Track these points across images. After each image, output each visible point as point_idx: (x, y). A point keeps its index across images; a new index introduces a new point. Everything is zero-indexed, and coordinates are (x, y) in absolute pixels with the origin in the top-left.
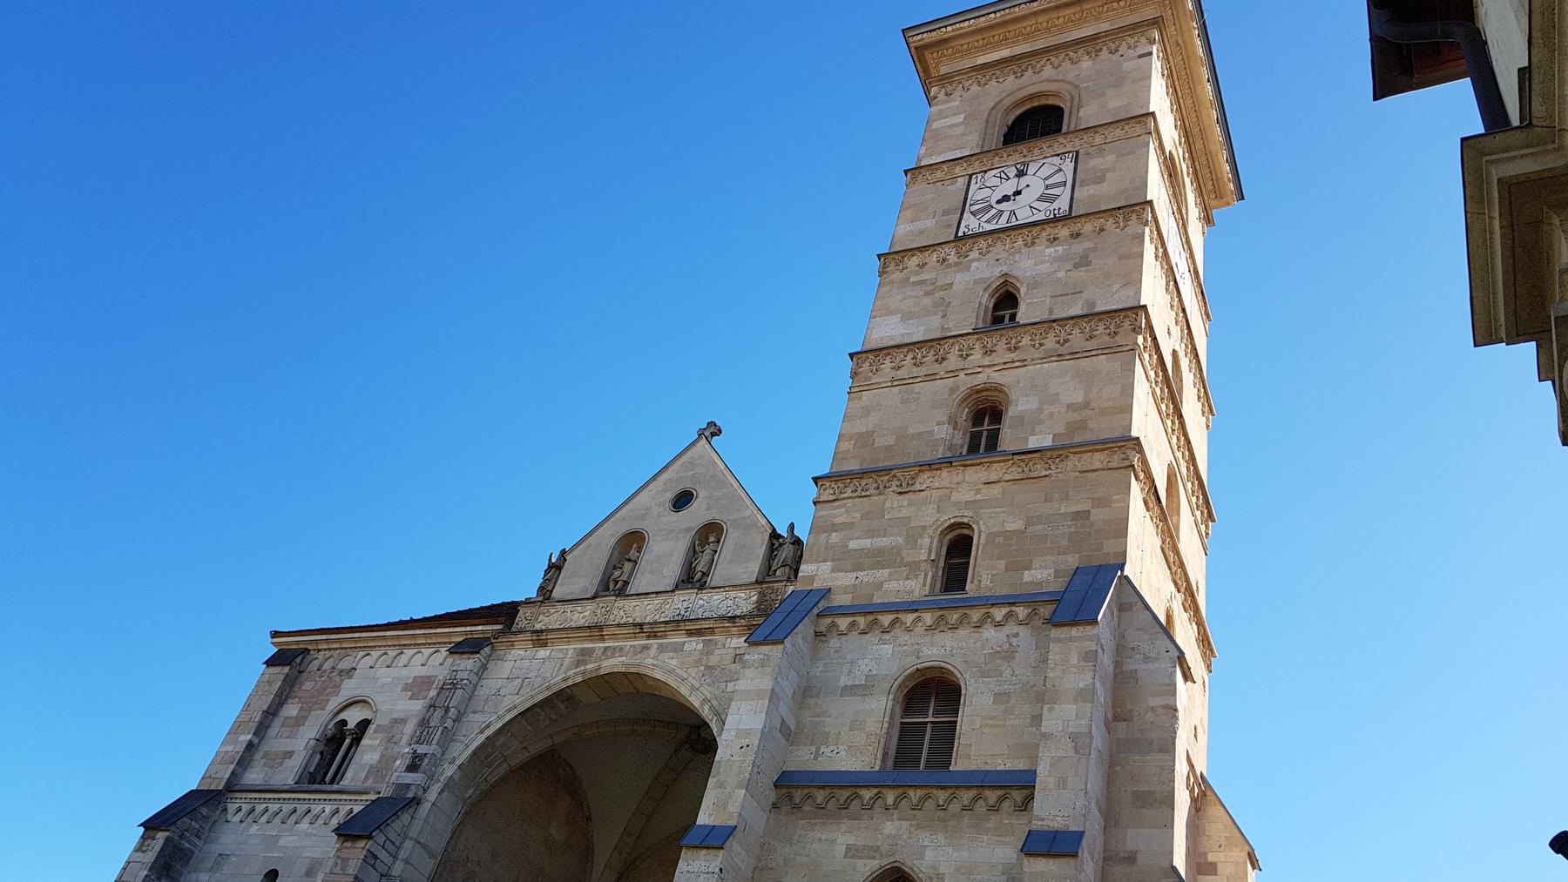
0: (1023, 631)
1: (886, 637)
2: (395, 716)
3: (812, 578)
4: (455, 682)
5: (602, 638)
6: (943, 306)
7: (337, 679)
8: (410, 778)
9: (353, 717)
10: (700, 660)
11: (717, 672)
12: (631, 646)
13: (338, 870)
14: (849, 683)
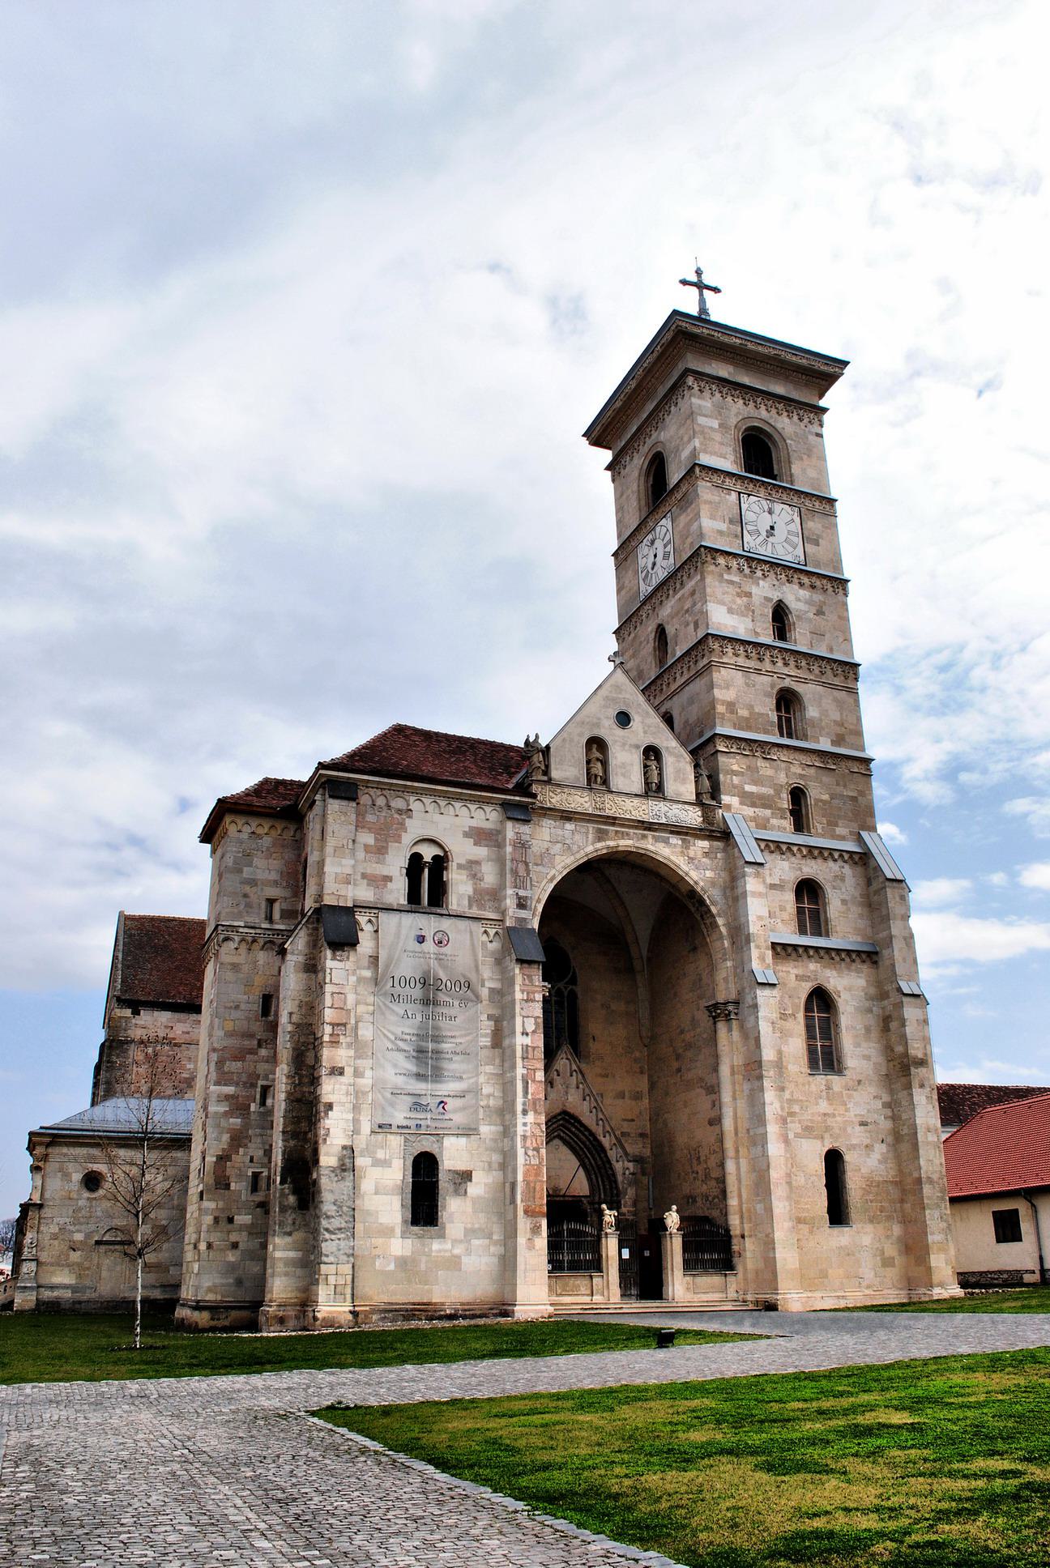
0: (847, 866)
1: (784, 857)
2: (470, 858)
3: (728, 807)
5: (613, 824)
6: (748, 610)
7: (396, 816)
8: (523, 914)
9: (428, 853)
10: (682, 852)
11: (696, 862)
13: (527, 982)
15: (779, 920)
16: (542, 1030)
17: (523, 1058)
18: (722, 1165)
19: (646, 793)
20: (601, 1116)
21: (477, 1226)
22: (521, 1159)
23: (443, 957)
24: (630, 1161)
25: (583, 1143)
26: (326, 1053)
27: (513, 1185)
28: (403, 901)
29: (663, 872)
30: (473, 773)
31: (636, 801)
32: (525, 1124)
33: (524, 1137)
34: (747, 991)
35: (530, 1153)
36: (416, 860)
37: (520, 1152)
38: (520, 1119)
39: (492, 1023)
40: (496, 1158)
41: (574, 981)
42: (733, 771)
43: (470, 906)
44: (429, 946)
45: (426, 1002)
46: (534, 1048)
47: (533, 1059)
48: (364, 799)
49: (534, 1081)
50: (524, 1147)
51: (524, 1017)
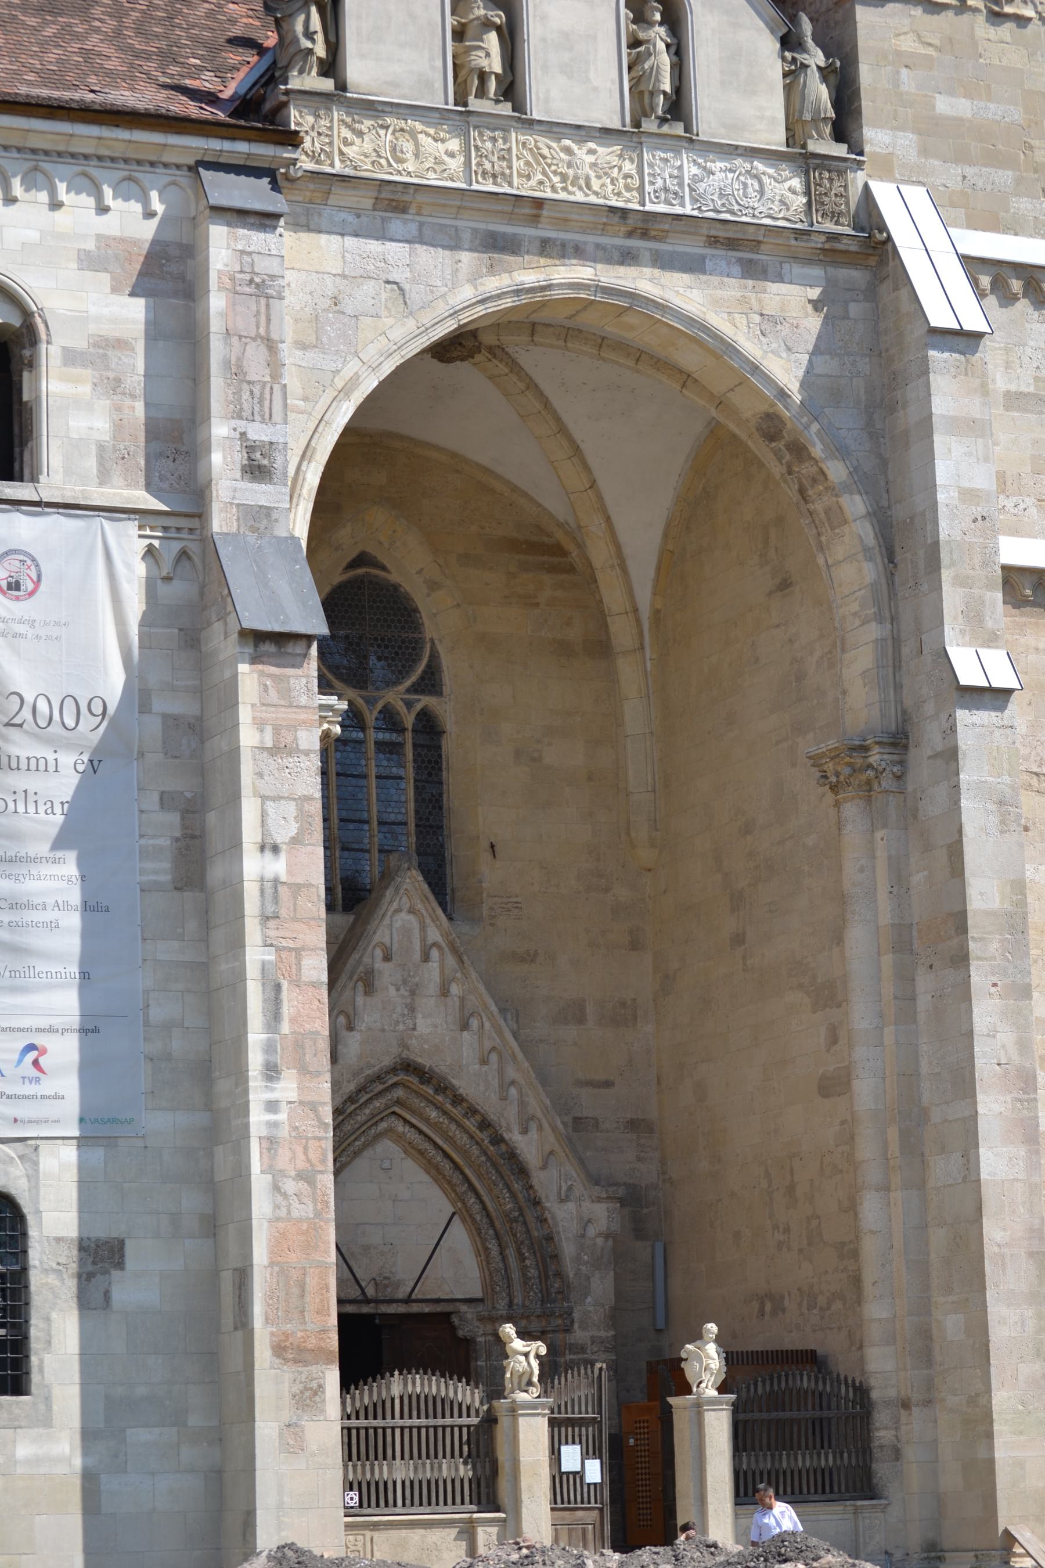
2: (92, 328)
4: (257, 280)
5: (535, 220)
8: (260, 494)
12: (598, 246)
13: (273, 696)
14: (1013, 388)
15: (1029, 501)
16: (318, 836)
17: (265, 919)
18: (852, 1208)
19: (637, 124)
20: (511, 1073)
21: (141, 1391)
22: (261, 1205)
23: (21, 629)
24: (599, 1200)
25: (465, 1153)
27: (243, 1276)
29: (689, 359)
30: (110, 74)
31: (601, 150)
32: (272, 1106)
33: (271, 1143)
34: (929, 708)
35: (290, 1186)
37: (259, 1183)
38: (258, 1094)
39: (174, 818)
40: (192, 1201)
41: (430, 683)
42: (899, 54)
43: (104, 477)
46: (296, 889)
47: (295, 919)
49: (296, 983)
50: (269, 1169)
51: (264, 798)
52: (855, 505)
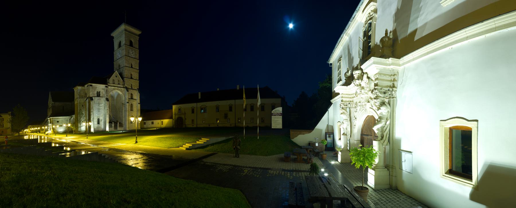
9: (98, 91)
26: (91, 110)
28: (96, 96)
36: (97, 92)
44: (99, 100)
45: (99, 105)
48: (93, 86)
52: (124, 97)
